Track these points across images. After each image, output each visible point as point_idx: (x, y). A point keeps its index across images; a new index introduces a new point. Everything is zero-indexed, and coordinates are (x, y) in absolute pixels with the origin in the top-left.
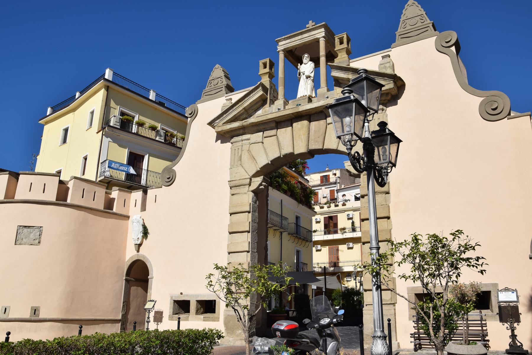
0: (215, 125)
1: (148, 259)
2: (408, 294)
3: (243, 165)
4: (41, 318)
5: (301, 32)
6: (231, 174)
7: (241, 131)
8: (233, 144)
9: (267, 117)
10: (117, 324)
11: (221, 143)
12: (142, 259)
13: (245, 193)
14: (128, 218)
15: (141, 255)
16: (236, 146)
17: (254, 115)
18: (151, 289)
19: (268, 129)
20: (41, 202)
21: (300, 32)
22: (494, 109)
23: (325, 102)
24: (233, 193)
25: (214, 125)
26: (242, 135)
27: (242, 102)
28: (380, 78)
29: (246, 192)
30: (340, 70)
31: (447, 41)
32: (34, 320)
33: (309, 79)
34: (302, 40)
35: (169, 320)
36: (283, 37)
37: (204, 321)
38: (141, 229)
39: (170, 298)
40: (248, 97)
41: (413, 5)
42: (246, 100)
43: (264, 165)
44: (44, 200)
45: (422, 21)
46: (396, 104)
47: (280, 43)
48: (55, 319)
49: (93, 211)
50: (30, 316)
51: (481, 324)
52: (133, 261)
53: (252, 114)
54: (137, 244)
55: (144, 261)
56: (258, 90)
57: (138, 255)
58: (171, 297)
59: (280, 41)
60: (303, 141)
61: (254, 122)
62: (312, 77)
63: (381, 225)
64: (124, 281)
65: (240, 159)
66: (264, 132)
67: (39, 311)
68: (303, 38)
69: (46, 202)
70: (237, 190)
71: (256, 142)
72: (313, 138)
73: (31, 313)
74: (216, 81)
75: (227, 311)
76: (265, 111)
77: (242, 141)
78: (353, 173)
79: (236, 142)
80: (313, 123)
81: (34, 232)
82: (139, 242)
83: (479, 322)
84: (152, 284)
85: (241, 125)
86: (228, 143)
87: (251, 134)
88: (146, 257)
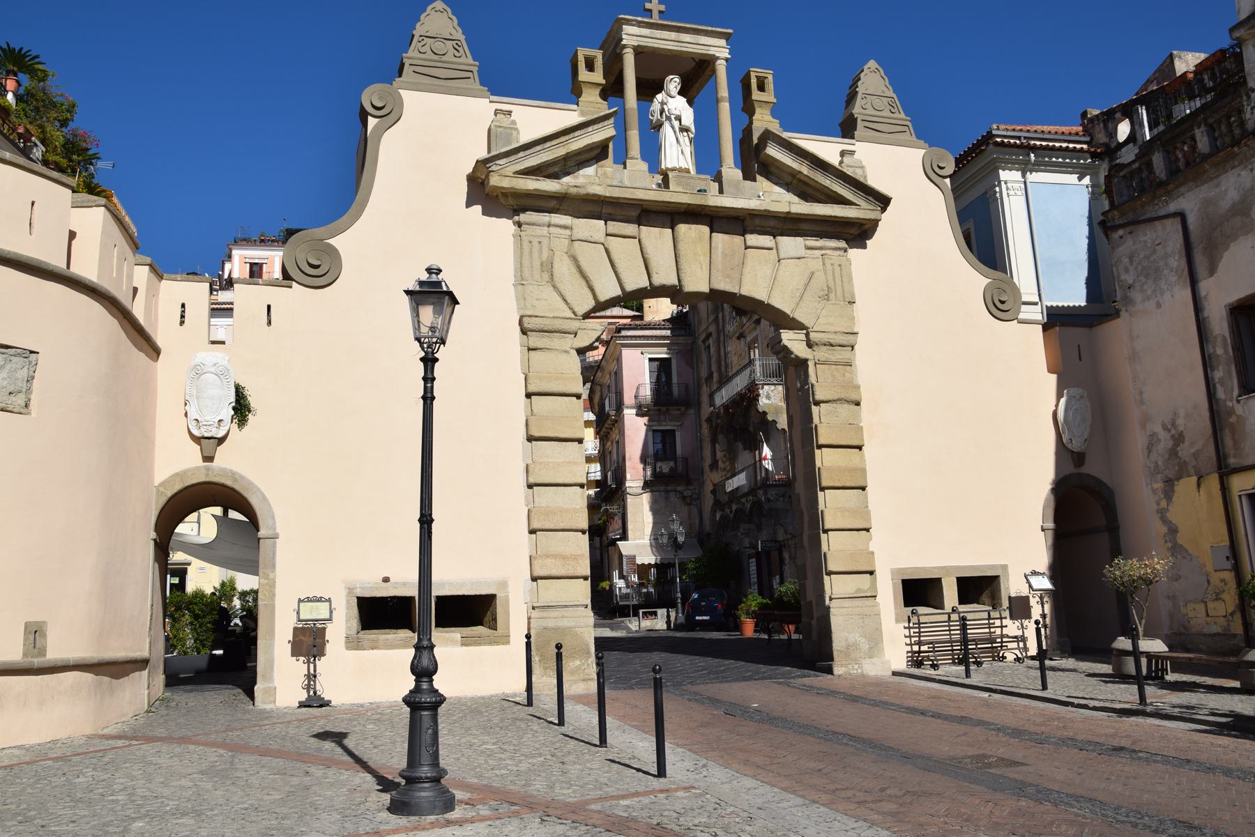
0: (493, 168)
1: (250, 483)
2: (892, 580)
3: (558, 285)
4: (50, 661)
5: (679, 27)
6: (521, 298)
7: (553, 204)
8: (524, 226)
9: (632, 193)
10: (143, 672)
11: (484, 214)
12: (229, 483)
13: (566, 352)
14: (155, 355)
15: (223, 470)
16: (533, 234)
17: (575, 174)
18: (274, 566)
19: (619, 217)
20: (35, 264)
21: (679, 25)
22: (1003, 302)
23: (761, 204)
24: (532, 345)
25: (490, 167)
26: (550, 212)
27: (567, 137)
28: (861, 194)
29: (568, 349)
30: (786, 149)
31: (941, 165)
32: (74, 664)
33: (685, 134)
34: (681, 44)
35: (347, 648)
36: (640, 19)
37: (463, 644)
38: (232, 398)
39: (344, 593)
40: (582, 131)
41: (876, 72)
42: (576, 135)
43: (611, 297)
44: (45, 262)
45: (893, 111)
46: (865, 247)
47: (627, 29)
48: (86, 662)
49: (125, 322)
50: (25, 655)
51: (989, 624)
52: (187, 484)
53: (570, 170)
54: (215, 436)
55: (237, 487)
56: (606, 123)
57: (208, 469)
58: (349, 589)
59: (628, 22)
60: (704, 268)
61: (600, 193)
62: (693, 134)
63: (850, 460)
64: (152, 542)
65: (548, 267)
66: (608, 222)
67: (44, 636)
68: (683, 42)
69: (51, 268)
70: (544, 340)
71: (590, 239)
72: (720, 267)
73: (24, 645)
74: (439, 46)
75: (540, 618)
76: (604, 174)
77: (549, 225)
78: (796, 356)
79: (533, 224)
80: (720, 235)
81: (8, 367)
82: (221, 434)
83: (987, 622)
84: (274, 554)
85: (563, 191)
86: (504, 220)
87: (571, 216)
88: (242, 477)
